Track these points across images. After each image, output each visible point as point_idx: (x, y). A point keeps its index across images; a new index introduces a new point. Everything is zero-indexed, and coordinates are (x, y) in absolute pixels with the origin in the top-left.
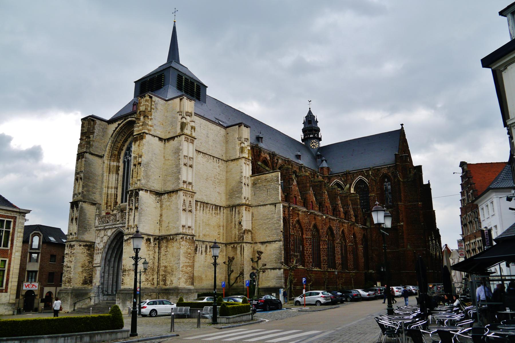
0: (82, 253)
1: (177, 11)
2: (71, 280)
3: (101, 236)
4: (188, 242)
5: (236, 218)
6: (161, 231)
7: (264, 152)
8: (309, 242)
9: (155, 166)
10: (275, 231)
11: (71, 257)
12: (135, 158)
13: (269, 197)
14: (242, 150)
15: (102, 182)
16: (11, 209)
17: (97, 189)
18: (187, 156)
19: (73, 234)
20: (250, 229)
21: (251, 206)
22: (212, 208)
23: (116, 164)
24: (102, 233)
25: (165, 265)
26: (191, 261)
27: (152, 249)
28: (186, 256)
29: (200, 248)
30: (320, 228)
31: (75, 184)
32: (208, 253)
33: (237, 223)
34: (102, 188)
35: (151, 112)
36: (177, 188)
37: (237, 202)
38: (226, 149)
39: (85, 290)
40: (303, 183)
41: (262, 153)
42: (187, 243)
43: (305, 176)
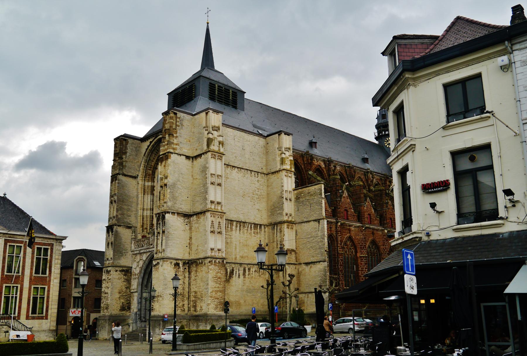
0: (119, 279)
1: (210, 10)
2: (108, 307)
3: (137, 261)
4: (218, 266)
5: (278, 237)
6: (190, 254)
7: (317, 160)
8: (364, 262)
9: (182, 186)
10: (319, 250)
11: (108, 283)
12: (162, 179)
13: (312, 213)
14: (282, 161)
15: (137, 204)
16: (47, 236)
17: (132, 211)
18: (214, 175)
19: (109, 259)
20: (294, 248)
21: (294, 223)
22: (251, 227)
23: (150, 185)
24: (138, 257)
26: (222, 286)
27: (182, 274)
28: (216, 281)
29: (237, 271)
30: (380, 244)
31: (110, 207)
32: (247, 276)
33: (279, 243)
34: (137, 210)
35: (175, 129)
36: (204, 209)
37: (279, 219)
38: (266, 161)
39: (123, 316)
40: (357, 194)
41: (315, 161)
42: (217, 267)
43: (358, 185)
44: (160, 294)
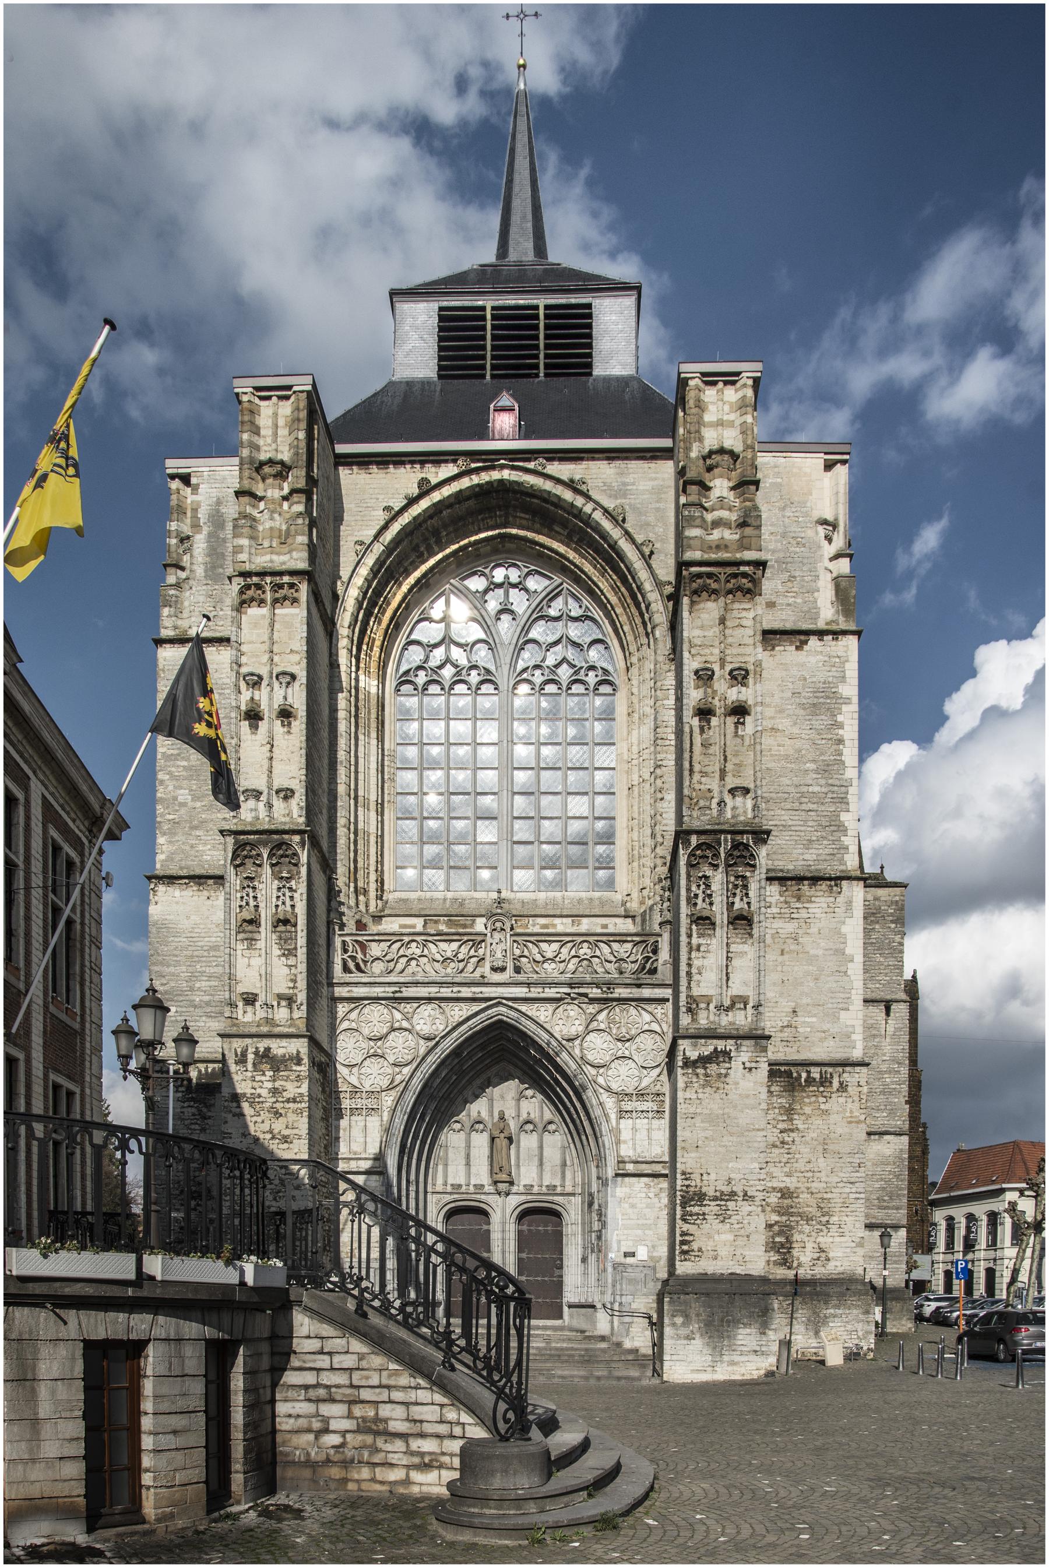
25: (782, 1185)
44: (738, 1189)
